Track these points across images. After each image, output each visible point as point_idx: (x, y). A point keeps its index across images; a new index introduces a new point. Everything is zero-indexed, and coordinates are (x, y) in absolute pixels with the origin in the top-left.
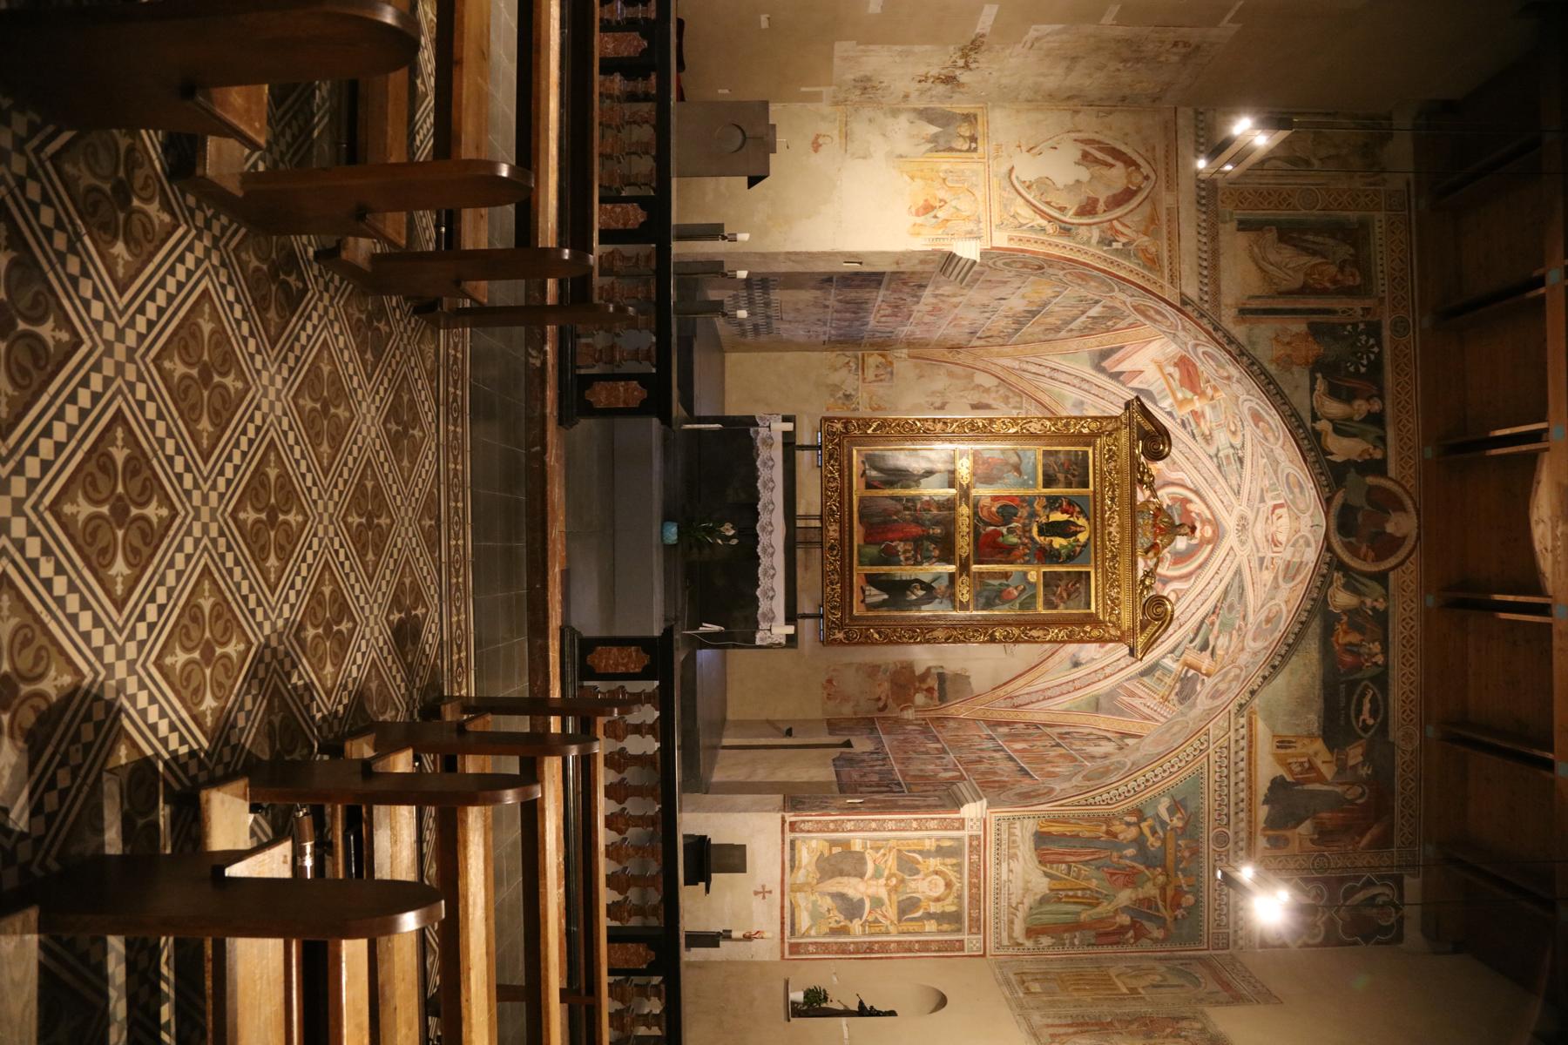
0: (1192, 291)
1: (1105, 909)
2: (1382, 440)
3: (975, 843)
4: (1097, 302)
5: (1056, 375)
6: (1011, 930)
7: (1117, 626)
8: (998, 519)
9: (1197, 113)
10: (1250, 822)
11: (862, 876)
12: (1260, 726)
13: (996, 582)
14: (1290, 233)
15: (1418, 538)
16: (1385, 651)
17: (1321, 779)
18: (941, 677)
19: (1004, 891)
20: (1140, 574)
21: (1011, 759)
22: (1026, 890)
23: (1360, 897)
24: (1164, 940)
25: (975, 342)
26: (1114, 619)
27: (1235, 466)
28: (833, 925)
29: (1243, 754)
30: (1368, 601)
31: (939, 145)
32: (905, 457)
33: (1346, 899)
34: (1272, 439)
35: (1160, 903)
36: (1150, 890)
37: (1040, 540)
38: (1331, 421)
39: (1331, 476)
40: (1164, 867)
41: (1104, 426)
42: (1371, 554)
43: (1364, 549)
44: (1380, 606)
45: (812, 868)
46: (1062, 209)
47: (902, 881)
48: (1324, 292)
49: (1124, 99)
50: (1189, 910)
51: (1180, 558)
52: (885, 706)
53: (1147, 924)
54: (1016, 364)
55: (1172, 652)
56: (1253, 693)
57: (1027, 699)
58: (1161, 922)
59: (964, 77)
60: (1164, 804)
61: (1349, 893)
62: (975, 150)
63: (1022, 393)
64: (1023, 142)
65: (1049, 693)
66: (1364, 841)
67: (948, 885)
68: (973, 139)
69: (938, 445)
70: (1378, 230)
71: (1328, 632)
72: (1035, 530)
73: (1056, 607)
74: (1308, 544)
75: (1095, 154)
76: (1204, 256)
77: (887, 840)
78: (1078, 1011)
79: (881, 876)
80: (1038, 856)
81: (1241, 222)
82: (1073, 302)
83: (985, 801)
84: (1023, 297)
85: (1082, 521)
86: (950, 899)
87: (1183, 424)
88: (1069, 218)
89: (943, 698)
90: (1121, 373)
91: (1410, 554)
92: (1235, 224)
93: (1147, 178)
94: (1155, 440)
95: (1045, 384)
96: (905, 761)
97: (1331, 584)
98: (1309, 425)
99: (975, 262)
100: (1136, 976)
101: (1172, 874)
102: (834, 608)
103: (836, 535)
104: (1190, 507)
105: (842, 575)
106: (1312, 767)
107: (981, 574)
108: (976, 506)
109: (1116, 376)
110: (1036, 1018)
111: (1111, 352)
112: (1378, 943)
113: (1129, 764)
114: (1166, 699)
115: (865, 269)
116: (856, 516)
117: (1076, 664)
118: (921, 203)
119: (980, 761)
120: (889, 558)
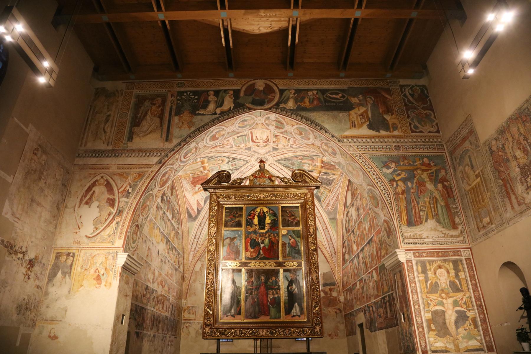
0: (156, 160)
1: (437, 195)
2: (225, 91)
3: (417, 255)
4: (164, 213)
5: (197, 236)
6: (455, 236)
7: (306, 195)
8: (257, 248)
9: (77, 157)
10: (388, 137)
11: (444, 312)
12: (347, 133)
13: (288, 249)
14: (136, 122)
15: (265, 79)
16: (312, 90)
17: (366, 112)
18: (325, 285)
19: (438, 240)
20: (283, 184)
21: (362, 250)
22: (435, 230)
23: (411, 98)
24: (445, 170)
25: (182, 270)
26: (303, 196)
27: (236, 162)
28: (472, 327)
29: (360, 140)
30: (291, 96)
31: (68, 272)
32: (225, 295)
33: (413, 103)
34: (223, 132)
35: (430, 172)
36: (425, 176)
37: (267, 229)
38: (216, 108)
39: (240, 107)
40: (414, 170)
41: (215, 201)
42: (272, 94)
43: (270, 97)
44: (293, 92)
45: (444, 339)
46: (110, 214)
47: (442, 290)
48: (163, 111)
49: (64, 185)
50: (430, 160)
52: (339, 309)
53: (440, 177)
54: (192, 253)
56: (333, 136)
58: (437, 172)
59: (31, 255)
60: (385, 170)
61: (409, 101)
62: (74, 254)
64: (75, 231)
65: (329, 239)
66: (387, 96)
67: (440, 267)
68: (68, 255)
69: (220, 277)
70: (141, 92)
71: (305, 109)
72: (262, 231)
73: (299, 221)
74: (268, 118)
75: (87, 198)
76: (141, 154)
77: (423, 299)
78: (498, 198)
79: (442, 302)
80: (418, 224)
81: (128, 140)
82: (163, 223)
83: (397, 250)
84: (158, 243)
85: (258, 210)
86: (447, 266)
88: (114, 211)
89: (333, 284)
90: (198, 209)
91: (272, 82)
92: (128, 142)
93: (102, 177)
94: (222, 177)
95: (201, 241)
96: (368, 297)
97: (285, 108)
98: (217, 116)
99: (128, 255)
100: (468, 177)
101: (416, 167)
102: (303, 332)
103: (265, 331)
105: (285, 328)
106: (362, 115)
107: (284, 257)
108: (250, 259)
109: (199, 212)
110: (509, 214)
111: (188, 212)
112: (428, 93)
113: (369, 187)
114: (330, 191)
115: (128, 314)
116: (255, 320)
118: (95, 282)
119: (365, 263)
120: (276, 302)
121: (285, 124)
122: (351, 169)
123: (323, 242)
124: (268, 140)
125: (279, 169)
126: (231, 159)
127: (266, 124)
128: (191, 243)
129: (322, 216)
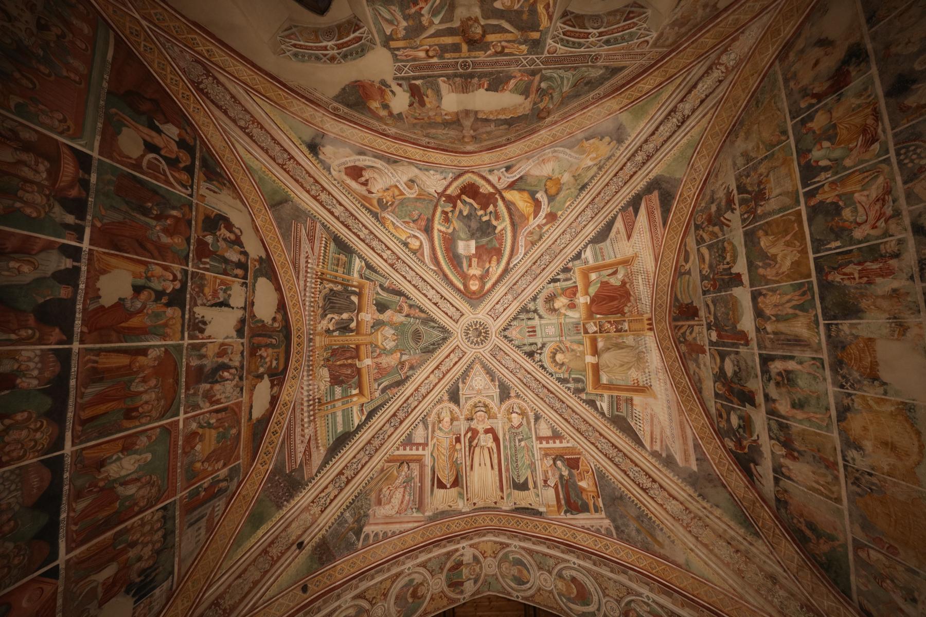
51: (450, 242)
55: (369, 266)
57: (226, 101)
63: (675, 47)
65: (256, 131)
74: (475, 582)
87: (566, 270)
90: (636, 211)
104: (494, 263)
109: (635, 203)
111: (666, 211)
114: (322, 278)
117: (314, 148)
121: (446, 589)
123: (268, 108)
124: (470, 442)
125: (442, 303)
126: (537, 357)
128: (710, 102)
129: (315, 198)
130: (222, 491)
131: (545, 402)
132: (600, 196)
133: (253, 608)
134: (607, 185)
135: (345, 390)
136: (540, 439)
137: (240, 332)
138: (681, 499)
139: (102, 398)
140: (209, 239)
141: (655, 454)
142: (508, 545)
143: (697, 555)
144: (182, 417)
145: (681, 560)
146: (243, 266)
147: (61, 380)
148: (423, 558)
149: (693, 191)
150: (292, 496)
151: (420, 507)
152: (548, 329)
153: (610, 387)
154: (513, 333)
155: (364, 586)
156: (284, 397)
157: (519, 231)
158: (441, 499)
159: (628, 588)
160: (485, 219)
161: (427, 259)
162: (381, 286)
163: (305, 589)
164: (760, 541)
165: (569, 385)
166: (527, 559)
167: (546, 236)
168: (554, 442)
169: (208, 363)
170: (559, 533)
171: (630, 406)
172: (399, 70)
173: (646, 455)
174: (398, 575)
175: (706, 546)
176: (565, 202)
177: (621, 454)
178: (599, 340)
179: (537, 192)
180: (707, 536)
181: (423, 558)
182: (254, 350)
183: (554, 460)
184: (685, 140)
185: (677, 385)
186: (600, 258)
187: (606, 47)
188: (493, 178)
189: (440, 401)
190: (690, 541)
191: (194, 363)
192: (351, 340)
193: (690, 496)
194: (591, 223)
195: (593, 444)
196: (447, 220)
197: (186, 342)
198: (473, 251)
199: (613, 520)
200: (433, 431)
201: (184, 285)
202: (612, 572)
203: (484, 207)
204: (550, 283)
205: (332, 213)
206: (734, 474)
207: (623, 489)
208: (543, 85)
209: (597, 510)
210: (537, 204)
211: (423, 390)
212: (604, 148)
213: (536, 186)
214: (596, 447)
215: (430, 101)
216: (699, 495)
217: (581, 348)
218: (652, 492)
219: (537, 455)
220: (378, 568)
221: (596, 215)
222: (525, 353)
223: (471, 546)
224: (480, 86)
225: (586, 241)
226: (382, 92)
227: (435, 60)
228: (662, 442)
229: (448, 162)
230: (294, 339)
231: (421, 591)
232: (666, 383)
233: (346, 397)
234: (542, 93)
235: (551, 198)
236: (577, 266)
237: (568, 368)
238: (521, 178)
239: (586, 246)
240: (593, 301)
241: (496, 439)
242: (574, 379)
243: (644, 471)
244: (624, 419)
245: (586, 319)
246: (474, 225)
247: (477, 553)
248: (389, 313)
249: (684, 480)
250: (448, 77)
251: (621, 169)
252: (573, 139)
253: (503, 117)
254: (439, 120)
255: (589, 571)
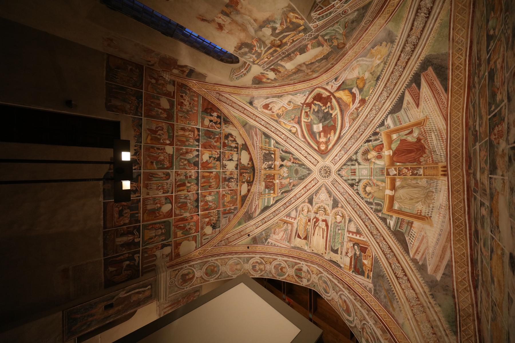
51: (309, 127)
55: (277, 142)
65: (234, 105)
74: (308, 281)
87: (375, 134)
90: (419, 86)
104: (332, 134)
109: (416, 80)
117: (251, 103)
121: (294, 275)
122: (238, 267)
126: (355, 187)
127: (309, 273)
129: (255, 120)
130: (232, 213)
131: (357, 213)
132: (390, 81)
133: (235, 245)
134: (392, 73)
135: (269, 191)
136: (349, 232)
137: (236, 168)
138: (418, 291)
139: (204, 182)
140: (226, 141)
141: (414, 261)
142: (322, 273)
143: (410, 323)
144: (221, 190)
145: (401, 321)
146: (237, 148)
147: (198, 177)
148: (286, 259)
149: (463, 58)
150: (249, 221)
151: (289, 241)
152: (363, 171)
153: (399, 212)
154: (343, 173)
155: (263, 256)
156: (252, 190)
157: (345, 114)
158: (298, 242)
159: (364, 317)
160: (326, 111)
161: (300, 136)
162: (282, 150)
163: (248, 247)
164: (455, 337)
165: (372, 206)
166: (329, 283)
167: (361, 114)
168: (356, 236)
169: (228, 176)
170: (347, 279)
171: (409, 227)
172: (263, 67)
173: (408, 259)
174: (276, 259)
175: (417, 321)
176: (369, 91)
177: (392, 254)
178: (397, 180)
179: (352, 88)
180: (421, 316)
181: (286, 259)
182: (241, 174)
183: (354, 245)
184: (437, 25)
185: (455, 220)
186: (398, 123)
187: (346, 5)
188: (328, 87)
189: (304, 202)
190: (410, 315)
191: (224, 176)
192: (272, 172)
193: (425, 292)
194: (388, 101)
195: (377, 243)
196: (307, 116)
197: (221, 170)
198: (321, 129)
199: (375, 286)
200: (299, 214)
201: (220, 155)
202: (361, 306)
203: (325, 104)
204: (365, 143)
205: (261, 124)
206: (468, 293)
207: (385, 272)
208: (326, 38)
209: (368, 277)
210: (354, 96)
211: (298, 196)
212: (384, 50)
213: (351, 85)
214: (379, 245)
215: (281, 69)
216: (431, 295)
217: (384, 185)
218: (401, 280)
219: (346, 239)
220: (270, 254)
221: (390, 94)
222: (349, 184)
223: (306, 265)
224: (296, 55)
225: (387, 113)
226: (264, 76)
227: (272, 58)
228: (423, 255)
229: (306, 86)
230: (256, 171)
231: (284, 270)
232: (444, 217)
233: (269, 193)
234: (330, 40)
235: (361, 90)
236: (383, 131)
237: (373, 196)
238: (343, 82)
239: (387, 117)
240: (394, 153)
241: (327, 225)
242: (376, 203)
243: (402, 267)
244: (403, 234)
245: (388, 166)
246: (321, 115)
247: (309, 269)
248: (286, 161)
249: (426, 282)
250: (281, 60)
251: (398, 60)
252: (366, 51)
253: (319, 58)
254: (291, 73)
255: (351, 300)
